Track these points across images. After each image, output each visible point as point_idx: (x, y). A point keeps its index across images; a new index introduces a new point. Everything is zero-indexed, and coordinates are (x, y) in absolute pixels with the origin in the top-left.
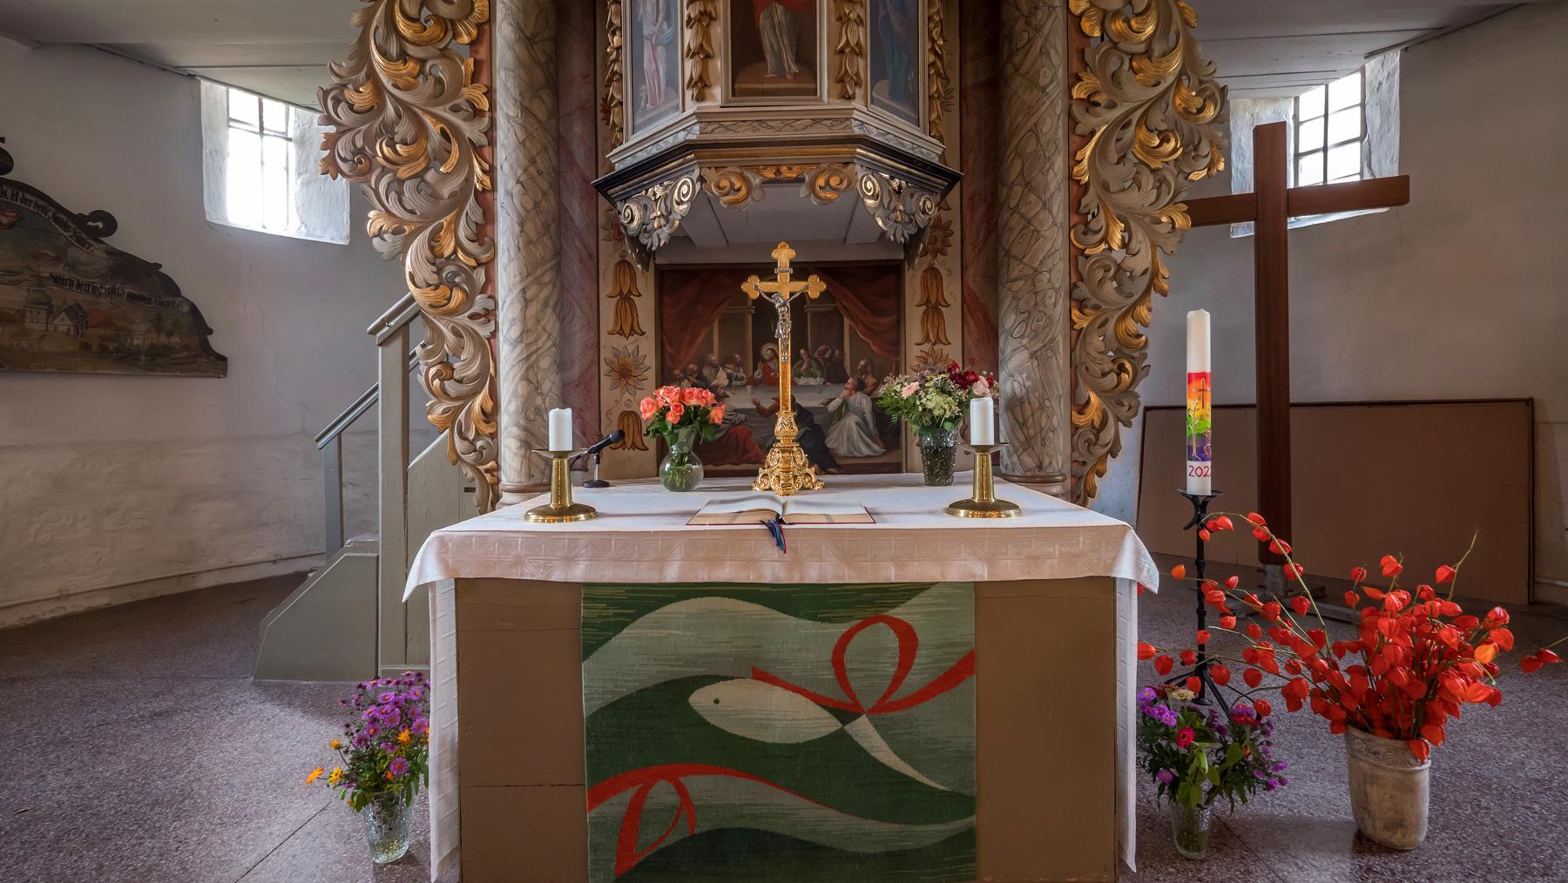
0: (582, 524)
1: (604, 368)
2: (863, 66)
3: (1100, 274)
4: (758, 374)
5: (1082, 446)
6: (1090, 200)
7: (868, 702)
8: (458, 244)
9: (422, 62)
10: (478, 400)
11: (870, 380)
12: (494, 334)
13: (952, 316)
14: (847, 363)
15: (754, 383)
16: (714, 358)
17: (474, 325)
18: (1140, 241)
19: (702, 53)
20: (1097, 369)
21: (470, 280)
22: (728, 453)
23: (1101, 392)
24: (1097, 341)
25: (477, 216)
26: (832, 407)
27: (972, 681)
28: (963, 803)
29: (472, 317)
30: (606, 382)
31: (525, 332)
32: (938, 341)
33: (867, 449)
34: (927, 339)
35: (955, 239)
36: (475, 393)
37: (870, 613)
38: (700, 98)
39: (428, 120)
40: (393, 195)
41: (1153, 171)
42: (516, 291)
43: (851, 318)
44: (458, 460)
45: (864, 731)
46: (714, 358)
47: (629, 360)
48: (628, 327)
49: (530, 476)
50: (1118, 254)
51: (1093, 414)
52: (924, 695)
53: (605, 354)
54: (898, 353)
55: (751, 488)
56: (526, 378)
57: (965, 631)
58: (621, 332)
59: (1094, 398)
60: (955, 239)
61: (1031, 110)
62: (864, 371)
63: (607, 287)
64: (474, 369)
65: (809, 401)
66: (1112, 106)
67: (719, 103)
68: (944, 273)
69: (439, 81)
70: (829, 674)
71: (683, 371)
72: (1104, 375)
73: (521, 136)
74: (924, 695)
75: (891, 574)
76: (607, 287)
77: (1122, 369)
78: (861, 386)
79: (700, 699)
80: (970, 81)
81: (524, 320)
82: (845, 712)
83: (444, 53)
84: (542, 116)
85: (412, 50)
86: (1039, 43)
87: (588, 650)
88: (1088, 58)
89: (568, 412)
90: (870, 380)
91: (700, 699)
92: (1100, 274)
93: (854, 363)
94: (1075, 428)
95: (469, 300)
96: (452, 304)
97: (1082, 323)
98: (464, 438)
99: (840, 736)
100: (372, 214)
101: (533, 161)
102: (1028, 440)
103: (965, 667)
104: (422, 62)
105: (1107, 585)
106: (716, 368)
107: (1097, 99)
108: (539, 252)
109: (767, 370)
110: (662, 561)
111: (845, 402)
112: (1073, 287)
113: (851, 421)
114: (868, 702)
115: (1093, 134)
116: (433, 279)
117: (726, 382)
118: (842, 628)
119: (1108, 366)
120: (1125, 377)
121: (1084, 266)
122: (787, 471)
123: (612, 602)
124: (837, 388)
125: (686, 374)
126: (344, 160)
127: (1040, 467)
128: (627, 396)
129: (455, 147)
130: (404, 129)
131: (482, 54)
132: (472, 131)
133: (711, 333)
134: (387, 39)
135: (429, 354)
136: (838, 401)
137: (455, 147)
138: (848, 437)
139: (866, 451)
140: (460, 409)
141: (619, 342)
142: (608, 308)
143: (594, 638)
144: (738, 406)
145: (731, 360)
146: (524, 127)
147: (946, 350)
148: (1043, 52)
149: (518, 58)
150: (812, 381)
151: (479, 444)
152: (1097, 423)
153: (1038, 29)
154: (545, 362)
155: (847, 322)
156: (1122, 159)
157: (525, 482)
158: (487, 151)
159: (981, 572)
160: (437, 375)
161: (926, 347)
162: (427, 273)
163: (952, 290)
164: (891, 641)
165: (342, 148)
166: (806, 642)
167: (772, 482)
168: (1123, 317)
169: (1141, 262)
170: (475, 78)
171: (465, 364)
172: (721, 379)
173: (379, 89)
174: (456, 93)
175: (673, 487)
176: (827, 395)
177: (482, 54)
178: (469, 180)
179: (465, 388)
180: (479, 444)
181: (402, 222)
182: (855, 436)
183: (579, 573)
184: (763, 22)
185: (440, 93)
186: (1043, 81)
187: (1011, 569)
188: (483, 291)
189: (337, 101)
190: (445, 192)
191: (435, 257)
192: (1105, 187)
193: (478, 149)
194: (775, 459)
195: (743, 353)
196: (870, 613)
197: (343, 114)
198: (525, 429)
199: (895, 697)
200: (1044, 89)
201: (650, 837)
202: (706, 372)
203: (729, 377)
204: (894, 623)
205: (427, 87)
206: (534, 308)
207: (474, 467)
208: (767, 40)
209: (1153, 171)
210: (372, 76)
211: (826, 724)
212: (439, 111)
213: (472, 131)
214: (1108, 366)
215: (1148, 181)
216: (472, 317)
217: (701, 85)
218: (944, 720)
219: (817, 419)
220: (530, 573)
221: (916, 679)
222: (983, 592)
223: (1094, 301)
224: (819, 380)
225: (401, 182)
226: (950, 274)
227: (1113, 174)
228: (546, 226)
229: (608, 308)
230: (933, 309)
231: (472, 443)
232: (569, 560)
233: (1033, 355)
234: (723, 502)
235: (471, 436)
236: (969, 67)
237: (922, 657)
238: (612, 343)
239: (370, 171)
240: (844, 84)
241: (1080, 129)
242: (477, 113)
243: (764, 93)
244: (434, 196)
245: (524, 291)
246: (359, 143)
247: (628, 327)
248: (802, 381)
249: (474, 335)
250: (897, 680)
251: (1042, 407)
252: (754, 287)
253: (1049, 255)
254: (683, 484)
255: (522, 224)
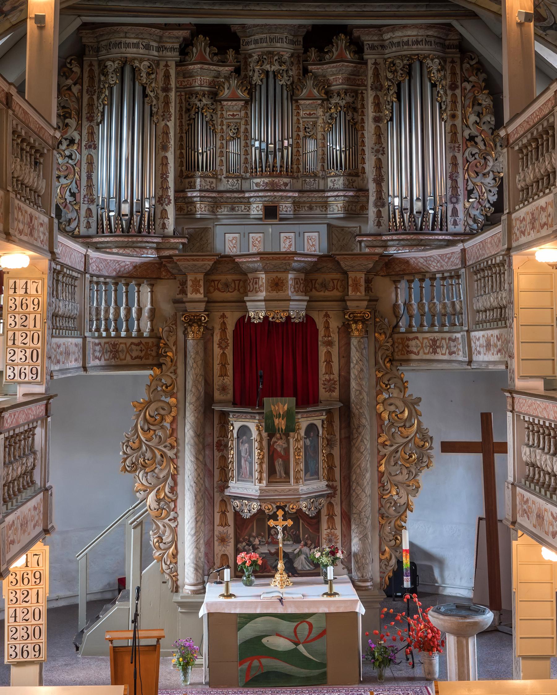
0: (233, 599)
1: (216, 538)
2: (302, 474)
3: (388, 505)
4: (270, 540)
5: (384, 567)
6: (384, 479)
7: (302, 641)
8: (165, 494)
9: (155, 431)
10: (171, 550)
11: (309, 542)
12: (177, 526)
13: (338, 519)
14: (301, 536)
15: (268, 543)
16: (254, 534)
17: (170, 523)
18: (403, 492)
19: (261, 472)
20: (388, 539)
21: (169, 507)
22: (264, 571)
23: (390, 547)
24: (388, 529)
25: (172, 484)
26: (296, 552)
27: (325, 636)
28: (324, 665)
29: (170, 520)
30: (216, 543)
31: (196, 532)
32: (333, 528)
33: (308, 567)
34: (329, 528)
35: (338, 492)
36: (170, 548)
37: (302, 620)
38: (260, 483)
39: (156, 451)
40: (144, 478)
41: (407, 468)
42: (194, 518)
43: (302, 519)
44: (163, 572)
45: (301, 648)
46: (254, 534)
47: (225, 536)
48: (224, 524)
49: (197, 580)
50: (396, 497)
51: (387, 555)
52: (314, 639)
53: (216, 533)
54: (319, 532)
55: (269, 585)
56: (196, 547)
57: (323, 624)
58: (222, 525)
59: (387, 548)
60: (338, 492)
61: (358, 459)
62: (307, 539)
63: (217, 509)
64: (170, 539)
65: (288, 550)
66: (391, 446)
67: (265, 485)
68: (334, 504)
69: (160, 437)
70: (293, 634)
71: (243, 539)
72: (390, 541)
73: (196, 467)
74: (314, 639)
75: (306, 611)
76: (217, 509)
77: (397, 539)
78: (306, 545)
79: (264, 641)
80: (343, 436)
81: (196, 528)
82: (297, 644)
83: (162, 427)
84: (201, 459)
85: (152, 427)
86: (360, 438)
87: (239, 629)
88: (383, 428)
89: (229, 570)
90: (309, 542)
91: (264, 641)
92: (388, 505)
93: (304, 535)
94: (381, 560)
95: (168, 514)
96: (163, 515)
97: (383, 522)
98: (166, 564)
99: (296, 649)
100: (136, 484)
101: (199, 475)
102: (359, 567)
103: (324, 633)
104: (155, 431)
105: (356, 613)
106: (255, 537)
107: (386, 443)
108: (201, 505)
109: (273, 539)
110: (256, 608)
111: (300, 550)
112: (380, 509)
113: (303, 557)
114: (302, 641)
115: (385, 455)
116: (157, 507)
117: (258, 543)
118: (296, 624)
119: (391, 538)
120: (398, 541)
121: (383, 502)
122: (281, 581)
123: (245, 618)
124: (297, 545)
125: (244, 540)
126: (128, 467)
127: (363, 576)
128: (224, 548)
129: (165, 460)
130: (148, 455)
131: (174, 427)
132: (170, 454)
133: (253, 525)
134: (144, 424)
135: (155, 534)
136: (298, 550)
137: (165, 460)
138: (300, 563)
139: (308, 568)
140: (164, 554)
141: (221, 529)
142: (217, 516)
143: (240, 627)
144: (263, 551)
145: (260, 535)
146: (196, 464)
147: (336, 531)
148: (362, 441)
149: (195, 442)
150: (289, 543)
151: (171, 566)
152: (389, 558)
153: (360, 434)
154: (202, 541)
155: (301, 521)
156: (396, 464)
157: (195, 582)
158: (175, 461)
159: (327, 610)
160: (158, 541)
161: (329, 531)
162: (154, 505)
163: (337, 510)
164: (307, 626)
165: (128, 462)
166: (287, 627)
167: (277, 584)
168: (397, 520)
169: (403, 501)
170: (171, 435)
171: (167, 538)
172: (257, 542)
173: (141, 441)
174: (165, 441)
175: (246, 585)
176: (294, 547)
177: (174, 427)
178: (169, 471)
179: (167, 546)
180: (171, 566)
181: (147, 487)
182: (304, 562)
183: (238, 611)
184: (276, 463)
185: (160, 443)
186: (362, 450)
187: (333, 610)
188: (173, 511)
189: (127, 446)
190: (161, 476)
191: (158, 501)
192: (390, 474)
193: (172, 460)
194: (278, 576)
195: (264, 533)
196: (302, 620)
197: (129, 451)
198: (196, 565)
199: (308, 640)
200: (362, 453)
201: (253, 673)
202: (251, 539)
203: (260, 541)
204: (308, 623)
205: (156, 440)
206: (199, 523)
207: (168, 574)
208: (277, 468)
209: (407, 468)
210: (138, 436)
211: (293, 646)
212: (160, 447)
213: (170, 454)
214: (391, 538)
215: (405, 471)
216: (170, 520)
217: (260, 481)
218: (319, 645)
219: (291, 556)
220: (227, 611)
221: (312, 636)
222: (327, 615)
223: (386, 515)
224: (291, 542)
225: (147, 473)
226: (337, 504)
227: (393, 470)
228: (202, 495)
229: (217, 516)
230: (331, 517)
231: (169, 566)
232: (235, 608)
233: (360, 539)
234: (267, 593)
235: (168, 563)
236: (343, 431)
237: (314, 630)
238: (218, 529)
239: (136, 470)
240: (297, 480)
241: (381, 454)
242: (172, 447)
243: (277, 482)
244: (158, 478)
245: (196, 518)
246: (134, 461)
247: (224, 524)
248: (285, 543)
249: (170, 526)
250: (308, 636)
251: (363, 557)
252: (272, 523)
253: (364, 507)
254: (249, 584)
255: (196, 496)
